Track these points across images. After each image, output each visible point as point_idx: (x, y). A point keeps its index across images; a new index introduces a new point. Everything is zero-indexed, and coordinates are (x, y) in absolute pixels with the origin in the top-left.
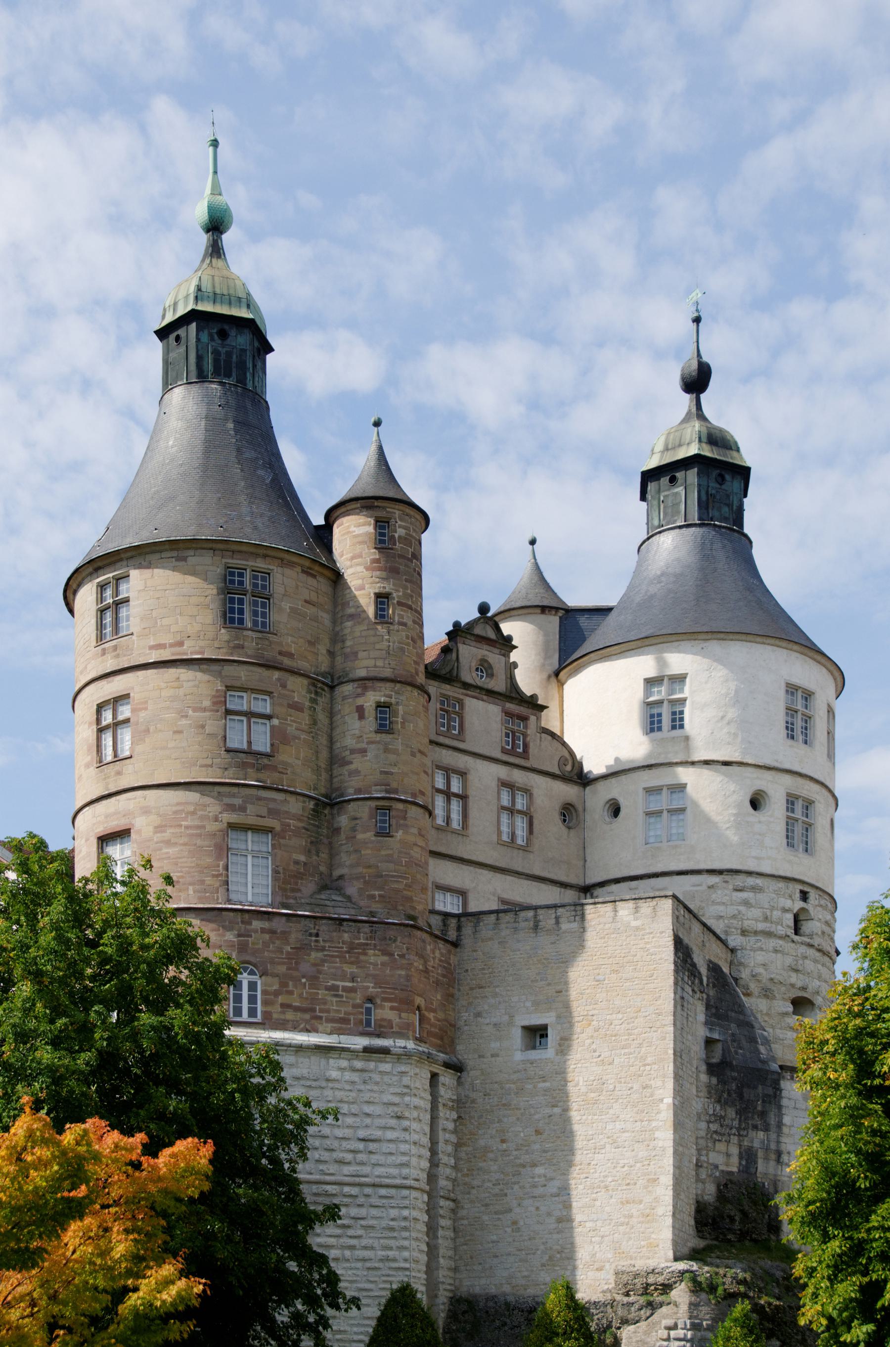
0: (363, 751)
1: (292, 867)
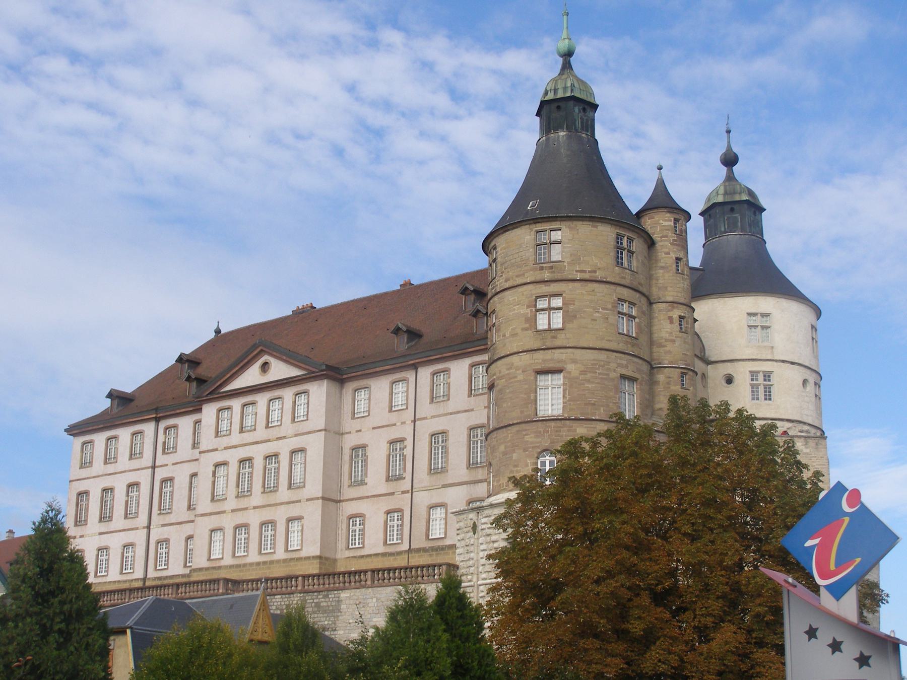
0: (673, 341)
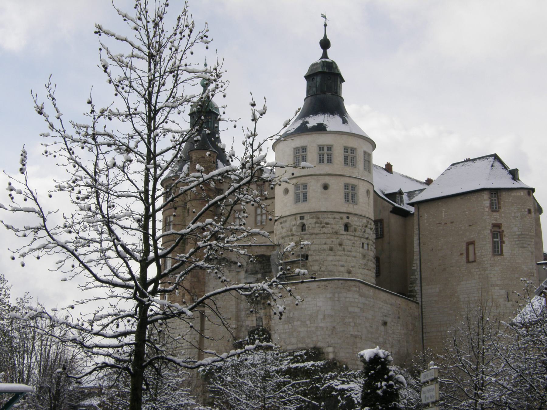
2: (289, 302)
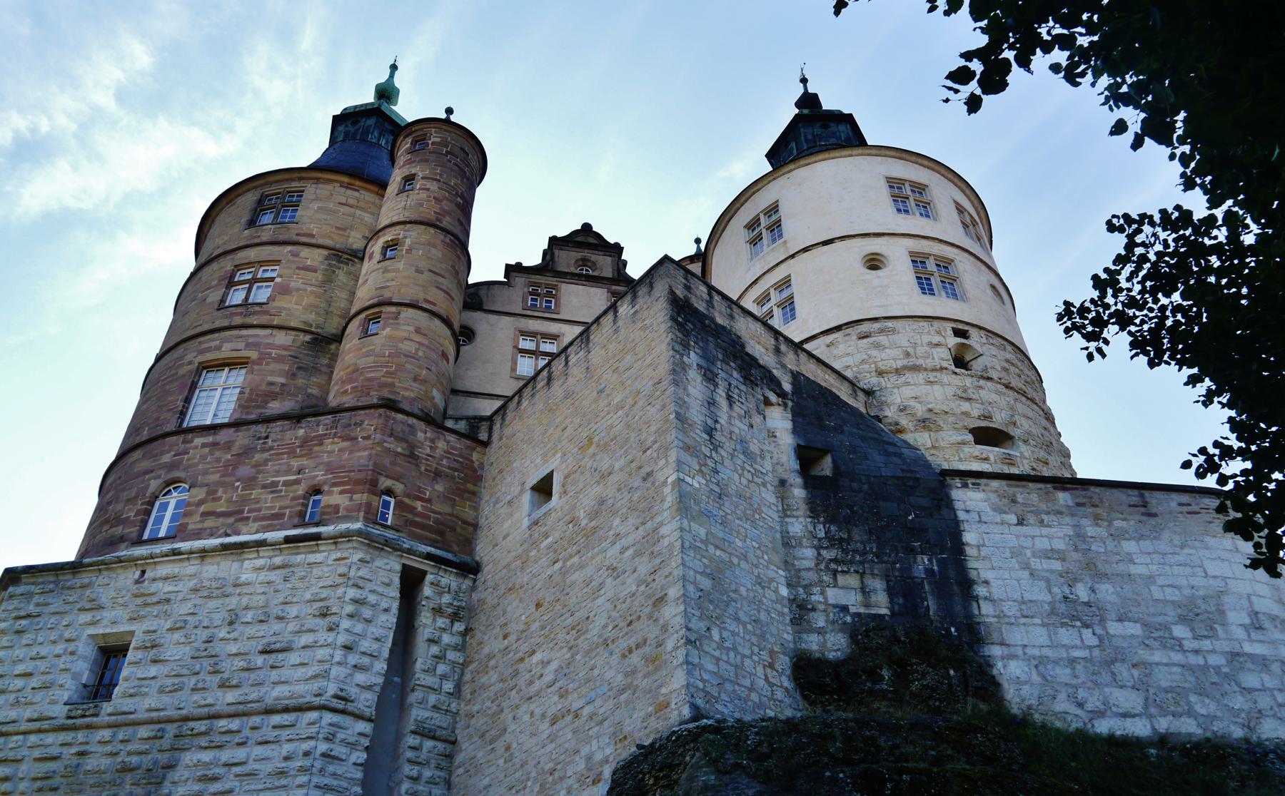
1: (264, 387)
2: (1060, 545)
